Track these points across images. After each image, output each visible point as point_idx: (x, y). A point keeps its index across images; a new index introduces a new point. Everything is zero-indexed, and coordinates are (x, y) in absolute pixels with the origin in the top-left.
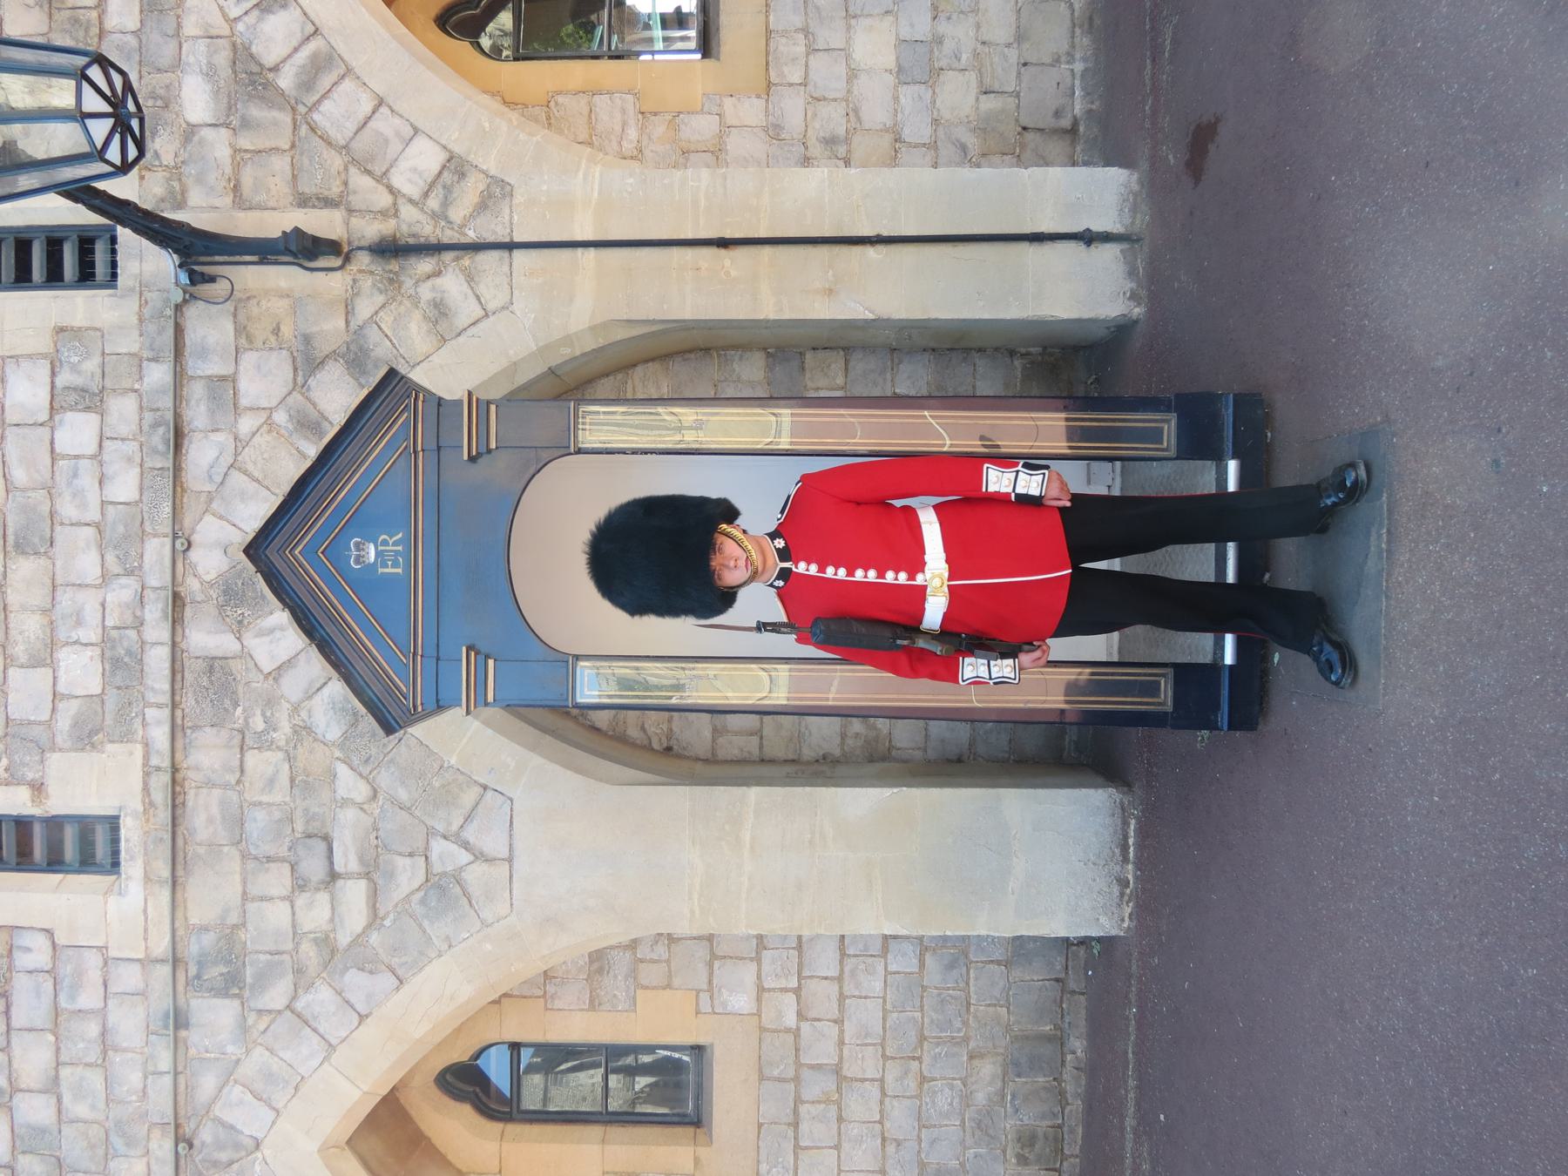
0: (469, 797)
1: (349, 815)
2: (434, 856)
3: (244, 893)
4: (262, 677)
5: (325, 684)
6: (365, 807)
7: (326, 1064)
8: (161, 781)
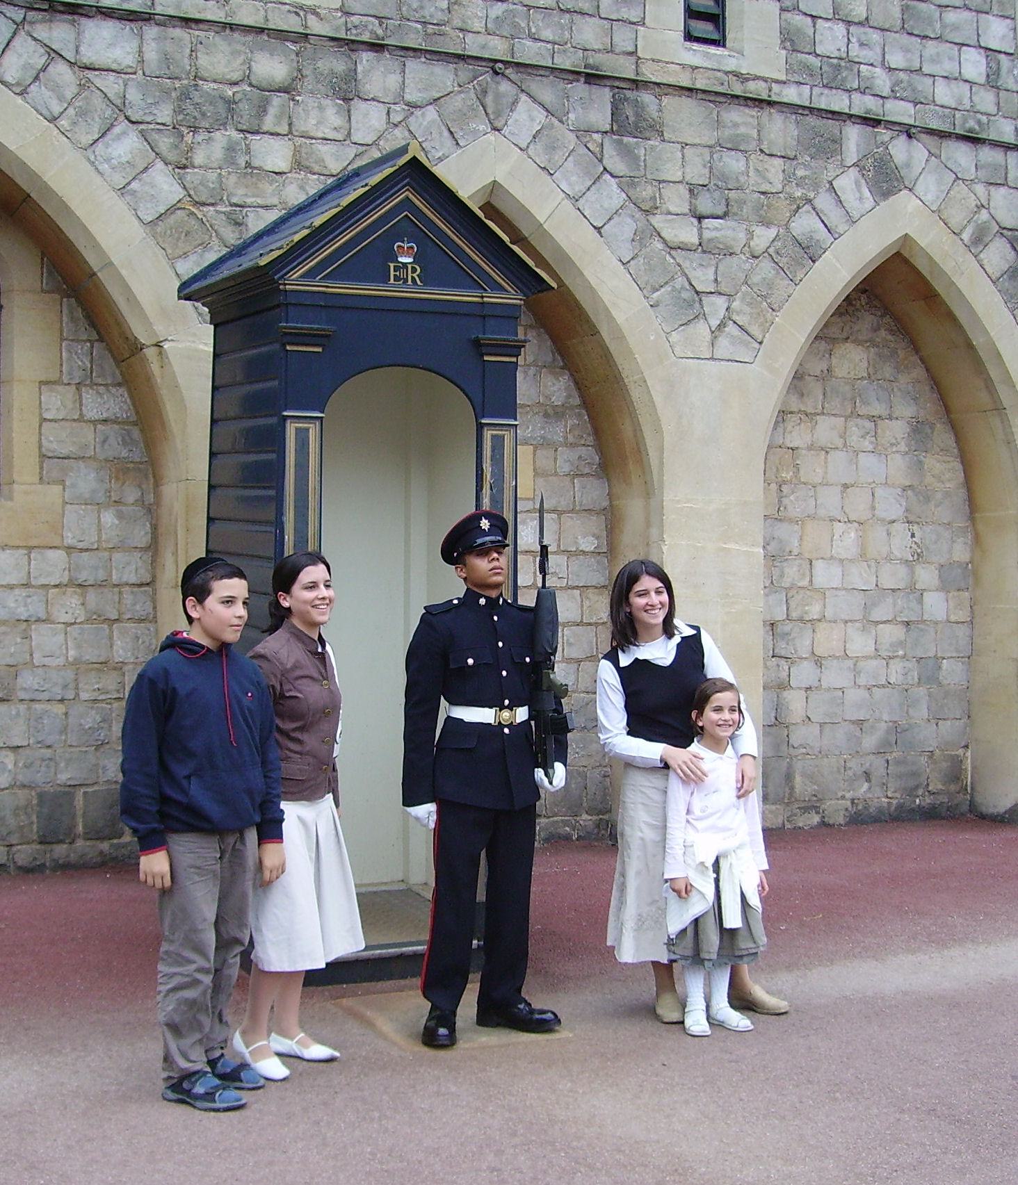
0: (755, 331)
1: (742, 236)
2: (713, 298)
3: (687, 145)
4: (830, 179)
5: (826, 226)
6: (746, 248)
7: (564, 195)
8: (756, 89)
